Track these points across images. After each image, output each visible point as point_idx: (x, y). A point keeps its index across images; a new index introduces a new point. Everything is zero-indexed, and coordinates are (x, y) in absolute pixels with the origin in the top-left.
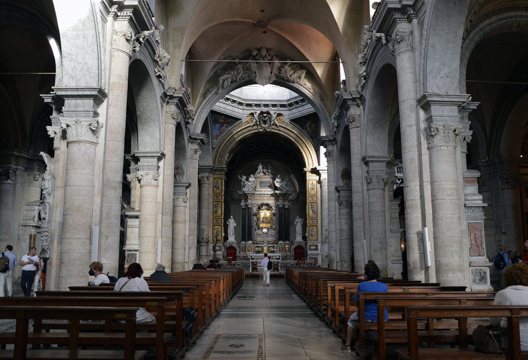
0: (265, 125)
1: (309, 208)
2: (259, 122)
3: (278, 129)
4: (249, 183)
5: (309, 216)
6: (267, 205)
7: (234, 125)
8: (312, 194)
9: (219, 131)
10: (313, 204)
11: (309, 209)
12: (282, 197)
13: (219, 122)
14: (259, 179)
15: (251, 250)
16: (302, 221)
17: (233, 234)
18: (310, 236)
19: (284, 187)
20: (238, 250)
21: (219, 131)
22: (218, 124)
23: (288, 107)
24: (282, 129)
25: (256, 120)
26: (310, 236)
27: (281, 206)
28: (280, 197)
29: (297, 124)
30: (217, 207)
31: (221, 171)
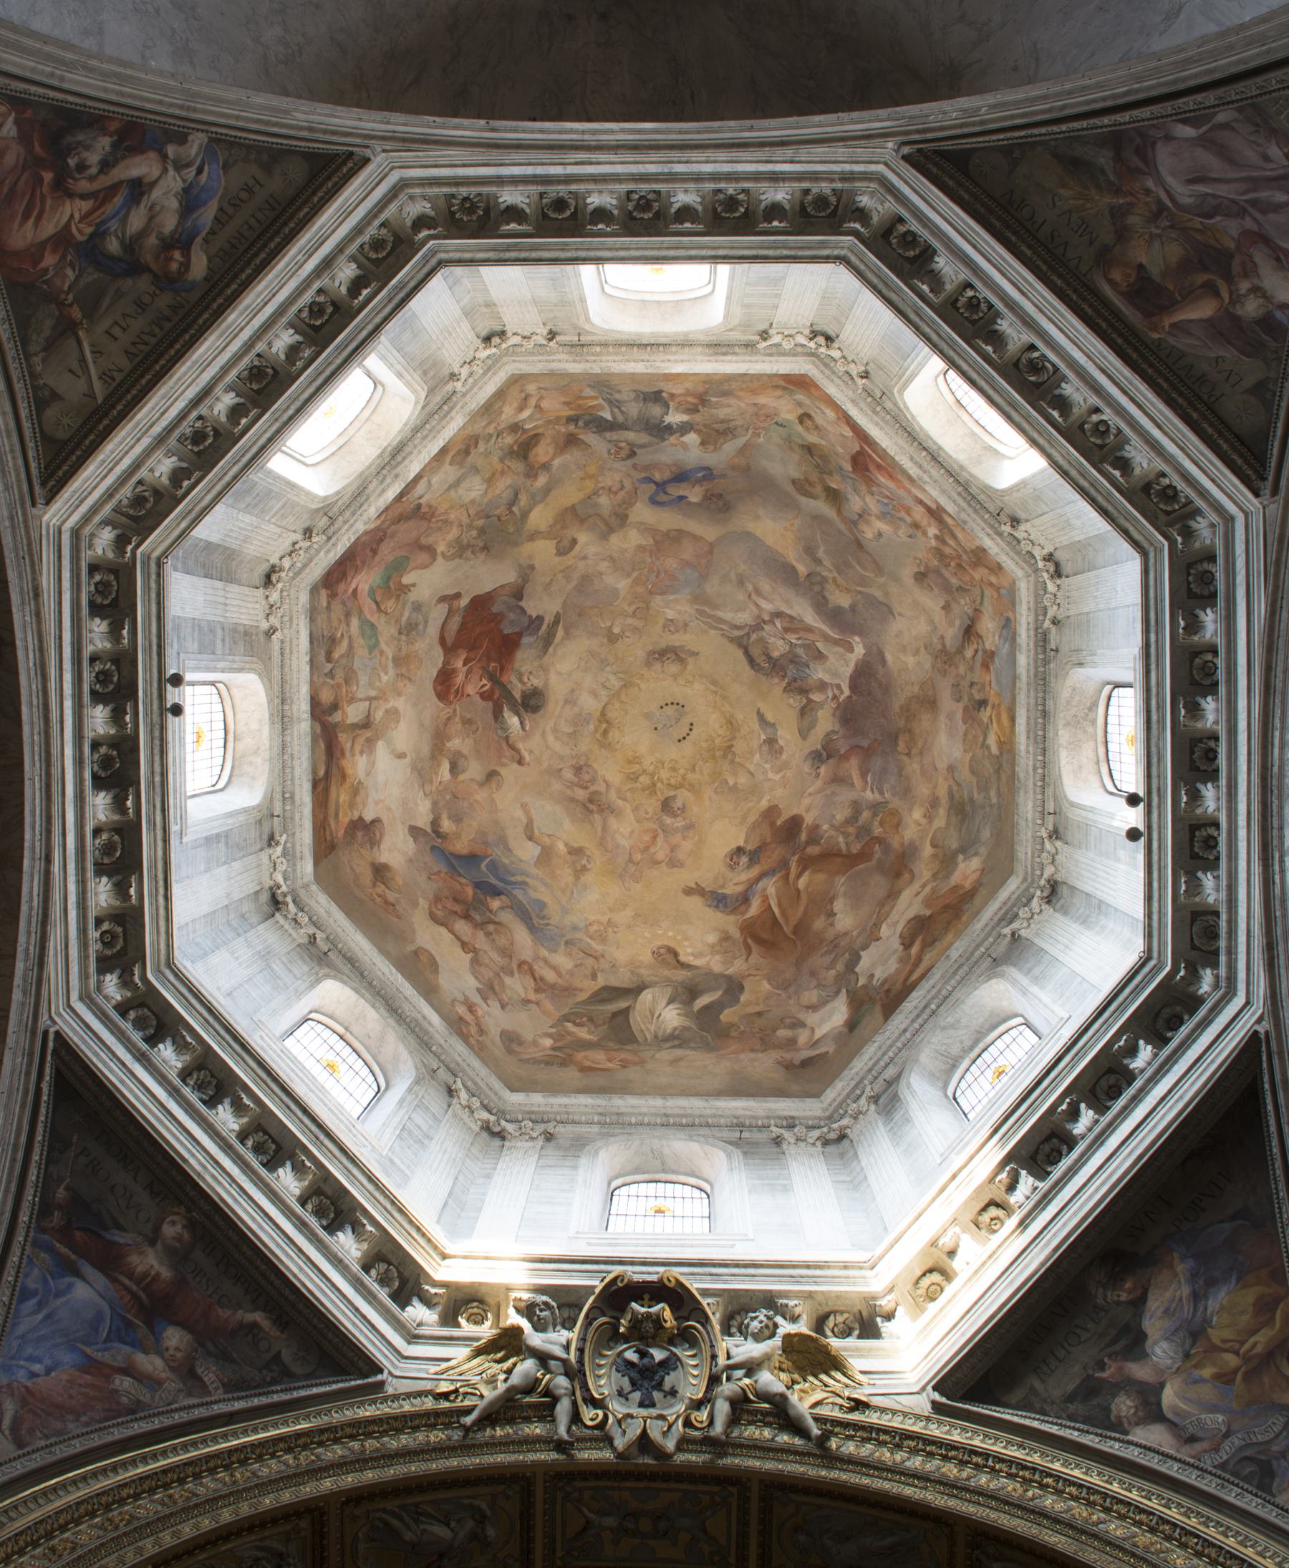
21: (91, 1366)
22: (100, 1279)
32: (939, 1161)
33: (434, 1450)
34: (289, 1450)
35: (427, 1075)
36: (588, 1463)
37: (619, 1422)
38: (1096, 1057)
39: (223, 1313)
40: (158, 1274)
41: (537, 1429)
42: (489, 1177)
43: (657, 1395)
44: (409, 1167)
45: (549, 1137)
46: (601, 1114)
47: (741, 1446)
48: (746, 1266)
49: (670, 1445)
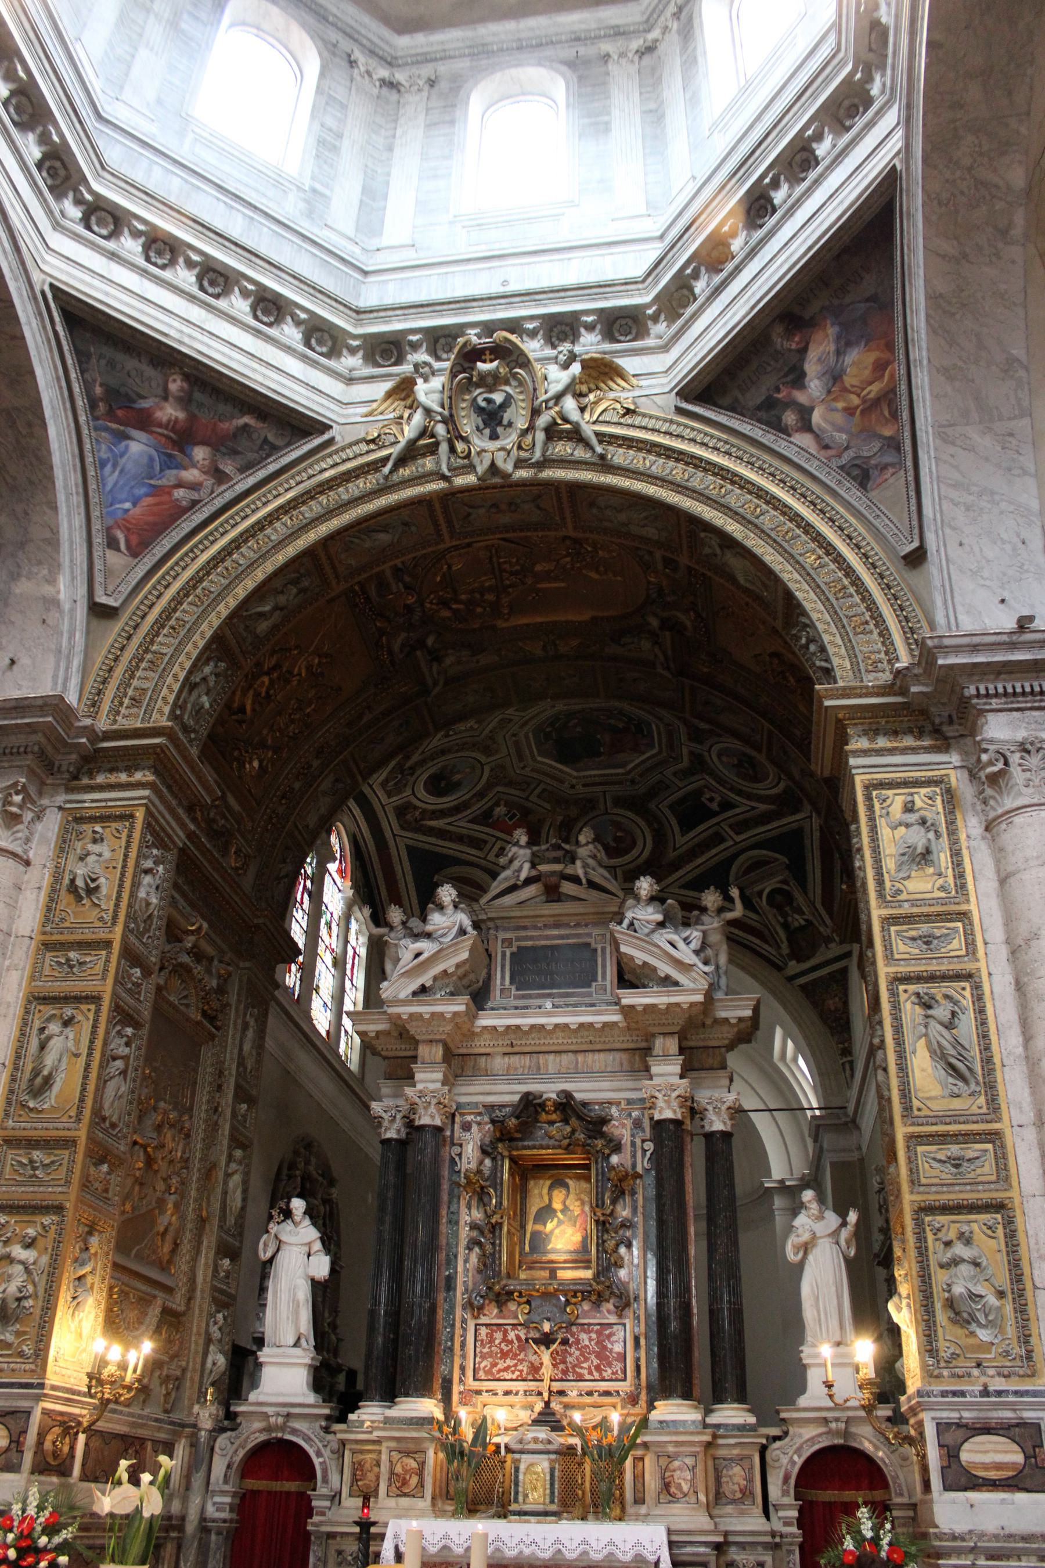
0: (494, 437)
1: (898, 1029)
2: (449, 421)
3: (587, 455)
4: (427, 947)
5: (907, 1108)
6: (567, 1106)
7: (272, 468)
8: (913, 903)
9: (156, 491)
10: (938, 990)
11: (899, 1042)
12: (672, 1045)
13: (144, 421)
14: (509, 935)
15: (421, 1484)
16: (845, 1234)
17: (297, 1344)
18: (942, 1316)
19: (690, 958)
20: (325, 1480)
21: (156, 491)
23: (660, 328)
24: (619, 456)
25: (428, 411)
26: (942, 1316)
27: (667, 1113)
28: (659, 1043)
29: (733, 409)
30: (52, 1042)
31: (129, 759)
32: (707, 134)
33: (370, 493)
34: (286, 513)
35: (329, 50)
36: (461, 486)
37: (479, 454)
38: (792, 140)
39: (225, 426)
40: (177, 418)
41: (428, 463)
42: (390, 149)
43: (499, 430)
44: (327, 186)
45: (432, 83)
46: (470, 47)
47: (554, 461)
48: (558, 291)
49: (509, 467)
